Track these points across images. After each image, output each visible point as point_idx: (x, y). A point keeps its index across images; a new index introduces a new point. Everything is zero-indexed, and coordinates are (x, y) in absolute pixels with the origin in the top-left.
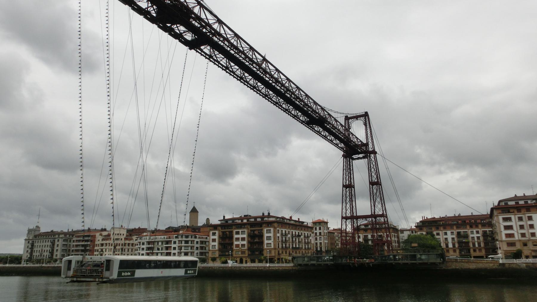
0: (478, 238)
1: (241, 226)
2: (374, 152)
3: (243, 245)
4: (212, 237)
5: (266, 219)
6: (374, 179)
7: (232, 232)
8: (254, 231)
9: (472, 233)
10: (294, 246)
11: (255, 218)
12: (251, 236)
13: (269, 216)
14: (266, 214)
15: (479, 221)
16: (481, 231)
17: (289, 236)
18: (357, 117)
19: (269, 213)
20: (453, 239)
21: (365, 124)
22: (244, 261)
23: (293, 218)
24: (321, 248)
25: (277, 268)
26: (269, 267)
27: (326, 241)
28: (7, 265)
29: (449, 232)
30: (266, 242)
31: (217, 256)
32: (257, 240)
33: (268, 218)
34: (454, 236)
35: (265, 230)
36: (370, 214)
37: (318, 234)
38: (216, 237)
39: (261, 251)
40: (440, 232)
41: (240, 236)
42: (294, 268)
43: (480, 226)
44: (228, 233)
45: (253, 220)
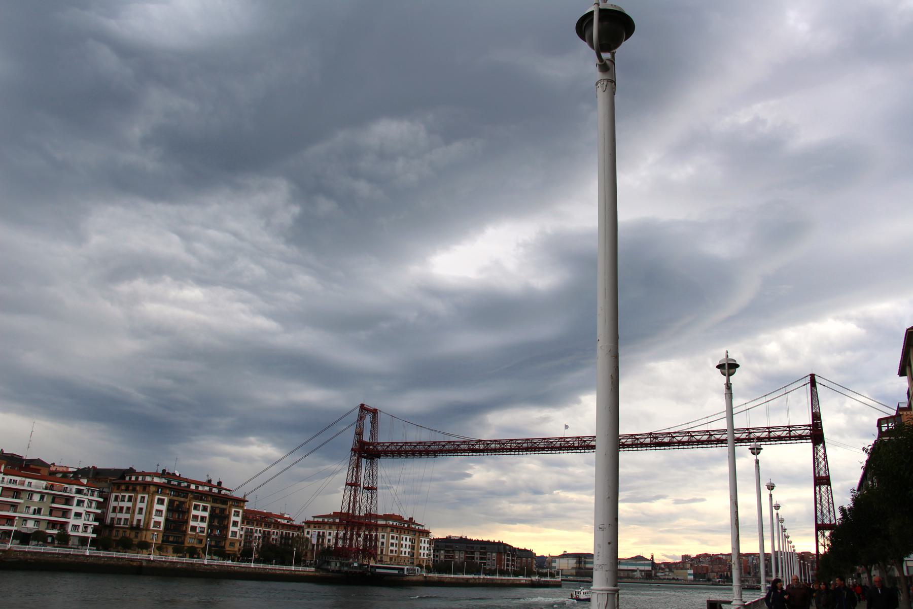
1: (201, 496)
4: (157, 507)
14: (214, 483)
18: (368, 410)
28: (482, 576)
38: (163, 508)
41: (200, 513)
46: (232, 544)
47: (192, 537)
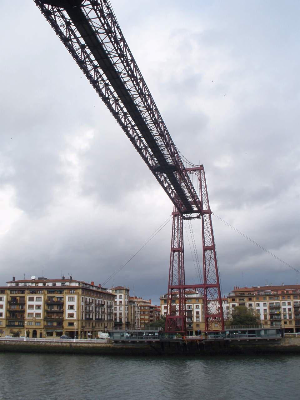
0: (290, 309)
2: (209, 212)
3: (38, 315)
5: (67, 284)
6: (208, 243)
7: (24, 297)
8: (52, 297)
9: (284, 304)
10: (97, 317)
11: (54, 282)
12: (49, 303)
13: (71, 280)
14: (67, 278)
15: (290, 292)
16: (292, 302)
17: (93, 305)
19: (71, 277)
20: (265, 310)
21: (200, 180)
22: (38, 335)
23: (95, 285)
24: (121, 319)
25: (86, 345)
26: (77, 343)
27: (127, 312)
29: (261, 303)
30: (67, 311)
31: (4, 326)
32: (55, 309)
33: (70, 282)
34: (266, 308)
36: (202, 282)
37: (118, 303)
39: (60, 323)
40: (253, 303)
41: (35, 303)
42: (108, 345)
43: (292, 297)
44: (18, 298)
45: (51, 284)
46: (71, 324)
47: (30, 321)
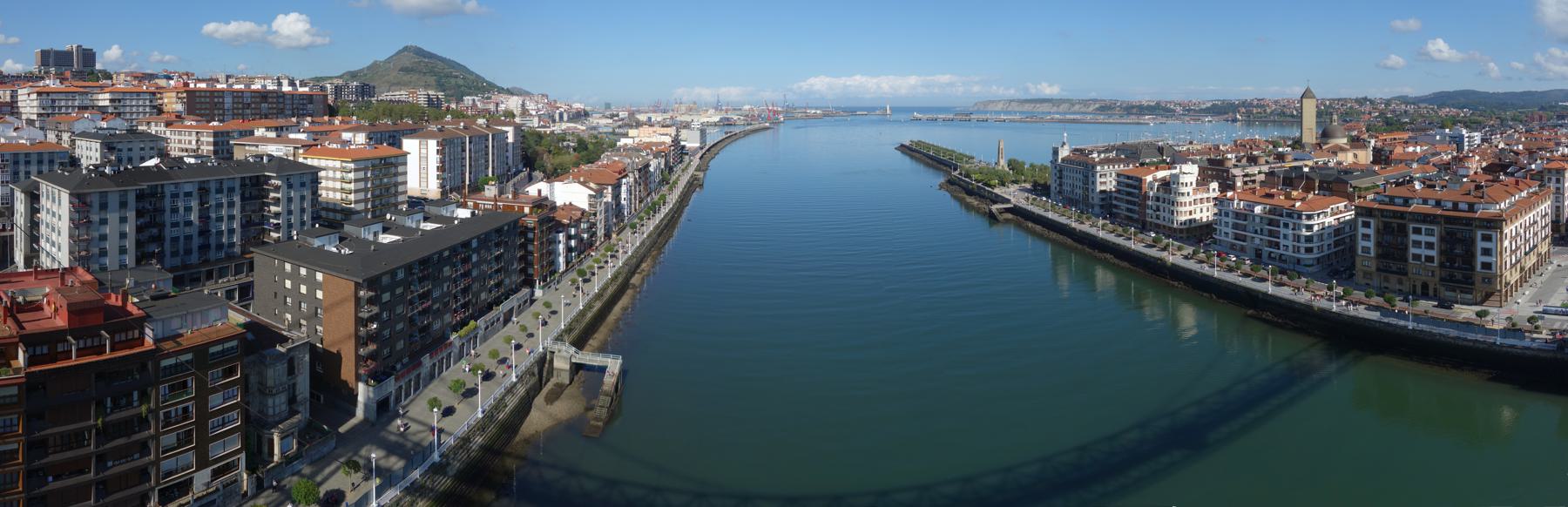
3: (1430, 259)
35: (1479, 234)
38: (1371, 231)
41: (1423, 238)
